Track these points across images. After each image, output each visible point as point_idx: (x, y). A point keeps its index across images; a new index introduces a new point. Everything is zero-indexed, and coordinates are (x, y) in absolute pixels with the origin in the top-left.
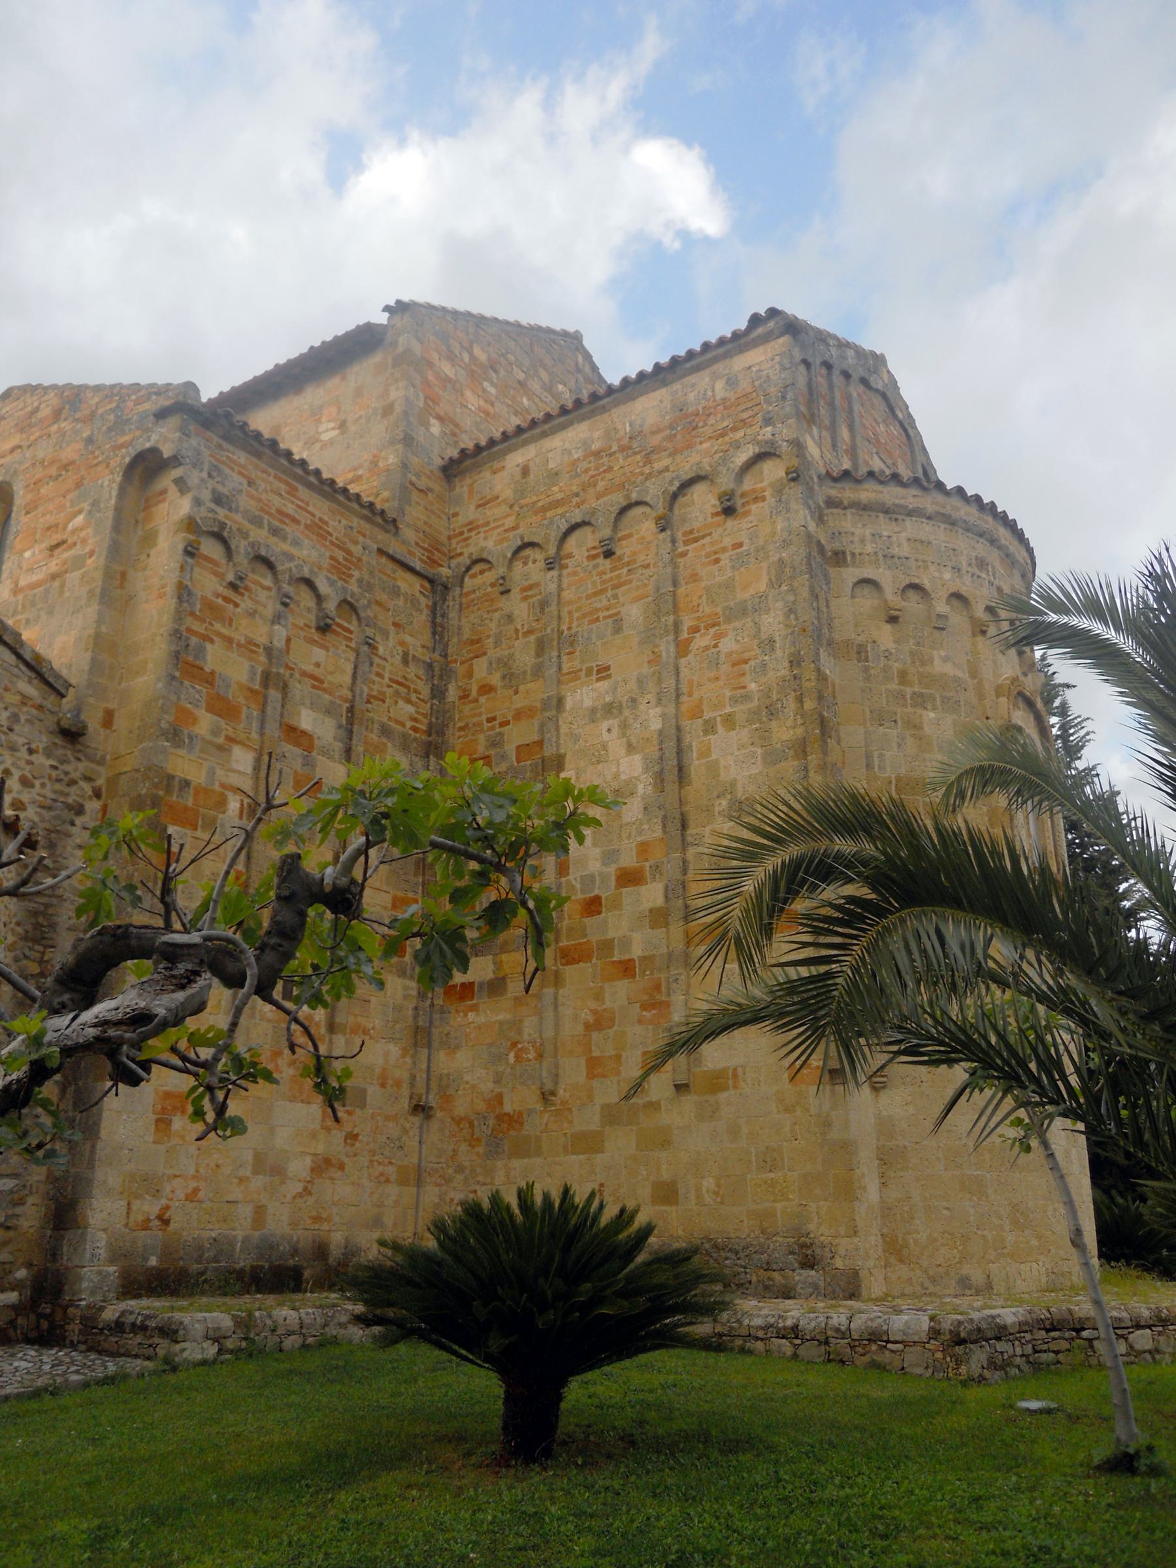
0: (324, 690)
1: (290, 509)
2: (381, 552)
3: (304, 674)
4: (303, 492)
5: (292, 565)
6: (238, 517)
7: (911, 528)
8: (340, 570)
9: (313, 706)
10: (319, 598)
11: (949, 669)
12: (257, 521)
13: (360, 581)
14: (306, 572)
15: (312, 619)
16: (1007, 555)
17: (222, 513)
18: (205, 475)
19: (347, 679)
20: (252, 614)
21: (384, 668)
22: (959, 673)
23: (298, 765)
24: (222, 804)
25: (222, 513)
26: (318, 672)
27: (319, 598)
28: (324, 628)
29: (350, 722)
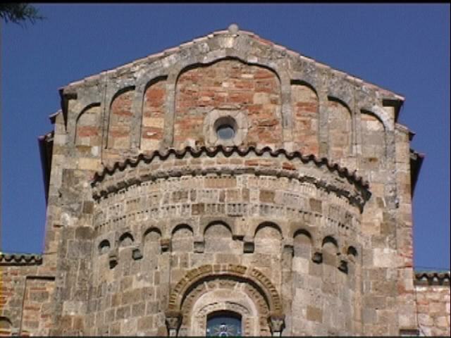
7: (133, 192)
11: (141, 284)
16: (219, 174)
22: (148, 285)
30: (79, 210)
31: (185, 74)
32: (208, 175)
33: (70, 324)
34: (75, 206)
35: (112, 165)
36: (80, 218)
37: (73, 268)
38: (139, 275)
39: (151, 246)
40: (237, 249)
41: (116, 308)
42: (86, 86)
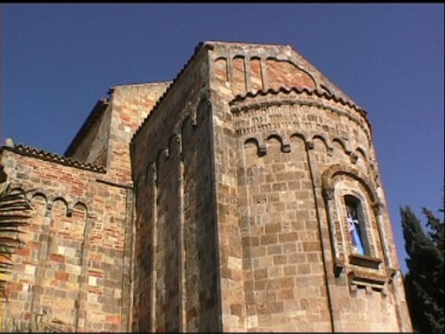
0: (71, 238)
1: (53, 174)
2: (98, 181)
3: (60, 233)
4: (59, 166)
5: (53, 194)
6: (29, 181)
7: (272, 110)
8: (76, 191)
9: (65, 245)
10: (66, 204)
11: (293, 169)
12: (37, 181)
13: (87, 194)
14: (60, 195)
15: (65, 212)
16: (333, 111)
18: (14, 169)
19: (82, 232)
21: (101, 225)
22: (298, 170)
23: (57, 269)
24: (20, 288)
25: (21, 181)
26: (67, 232)
27: (66, 204)
28: (69, 215)
29: (82, 248)
30: (223, 117)
31: (269, 62)
32: (327, 110)
33: (228, 191)
34: (221, 114)
35: (267, 88)
36: (225, 122)
37: (225, 153)
38: (290, 163)
39: (296, 146)
40: (347, 159)
41: (271, 184)
42: (219, 46)
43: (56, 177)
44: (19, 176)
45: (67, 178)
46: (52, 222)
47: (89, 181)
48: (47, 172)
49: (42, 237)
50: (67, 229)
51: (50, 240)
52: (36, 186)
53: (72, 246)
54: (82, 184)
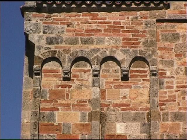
1: (94, 26)
2: (158, 21)
5: (98, 54)
6: (63, 45)
9: (124, 120)
12: (74, 42)
14: (108, 53)
17: (53, 47)
18: (41, 34)
20: (79, 87)
25: (53, 47)
26: (124, 101)
28: (125, 78)
43: (100, 31)
44: (50, 41)
45: (115, 28)
46: (103, 92)
47: (146, 24)
48: (85, 27)
49: (91, 116)
50: (125, 97)
51: (103, 118)
52: (74, 48)
53: (135, 120)
54: (137, 31)
